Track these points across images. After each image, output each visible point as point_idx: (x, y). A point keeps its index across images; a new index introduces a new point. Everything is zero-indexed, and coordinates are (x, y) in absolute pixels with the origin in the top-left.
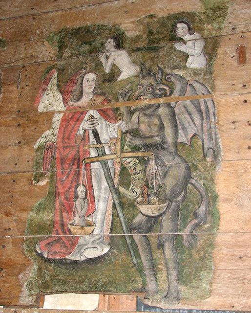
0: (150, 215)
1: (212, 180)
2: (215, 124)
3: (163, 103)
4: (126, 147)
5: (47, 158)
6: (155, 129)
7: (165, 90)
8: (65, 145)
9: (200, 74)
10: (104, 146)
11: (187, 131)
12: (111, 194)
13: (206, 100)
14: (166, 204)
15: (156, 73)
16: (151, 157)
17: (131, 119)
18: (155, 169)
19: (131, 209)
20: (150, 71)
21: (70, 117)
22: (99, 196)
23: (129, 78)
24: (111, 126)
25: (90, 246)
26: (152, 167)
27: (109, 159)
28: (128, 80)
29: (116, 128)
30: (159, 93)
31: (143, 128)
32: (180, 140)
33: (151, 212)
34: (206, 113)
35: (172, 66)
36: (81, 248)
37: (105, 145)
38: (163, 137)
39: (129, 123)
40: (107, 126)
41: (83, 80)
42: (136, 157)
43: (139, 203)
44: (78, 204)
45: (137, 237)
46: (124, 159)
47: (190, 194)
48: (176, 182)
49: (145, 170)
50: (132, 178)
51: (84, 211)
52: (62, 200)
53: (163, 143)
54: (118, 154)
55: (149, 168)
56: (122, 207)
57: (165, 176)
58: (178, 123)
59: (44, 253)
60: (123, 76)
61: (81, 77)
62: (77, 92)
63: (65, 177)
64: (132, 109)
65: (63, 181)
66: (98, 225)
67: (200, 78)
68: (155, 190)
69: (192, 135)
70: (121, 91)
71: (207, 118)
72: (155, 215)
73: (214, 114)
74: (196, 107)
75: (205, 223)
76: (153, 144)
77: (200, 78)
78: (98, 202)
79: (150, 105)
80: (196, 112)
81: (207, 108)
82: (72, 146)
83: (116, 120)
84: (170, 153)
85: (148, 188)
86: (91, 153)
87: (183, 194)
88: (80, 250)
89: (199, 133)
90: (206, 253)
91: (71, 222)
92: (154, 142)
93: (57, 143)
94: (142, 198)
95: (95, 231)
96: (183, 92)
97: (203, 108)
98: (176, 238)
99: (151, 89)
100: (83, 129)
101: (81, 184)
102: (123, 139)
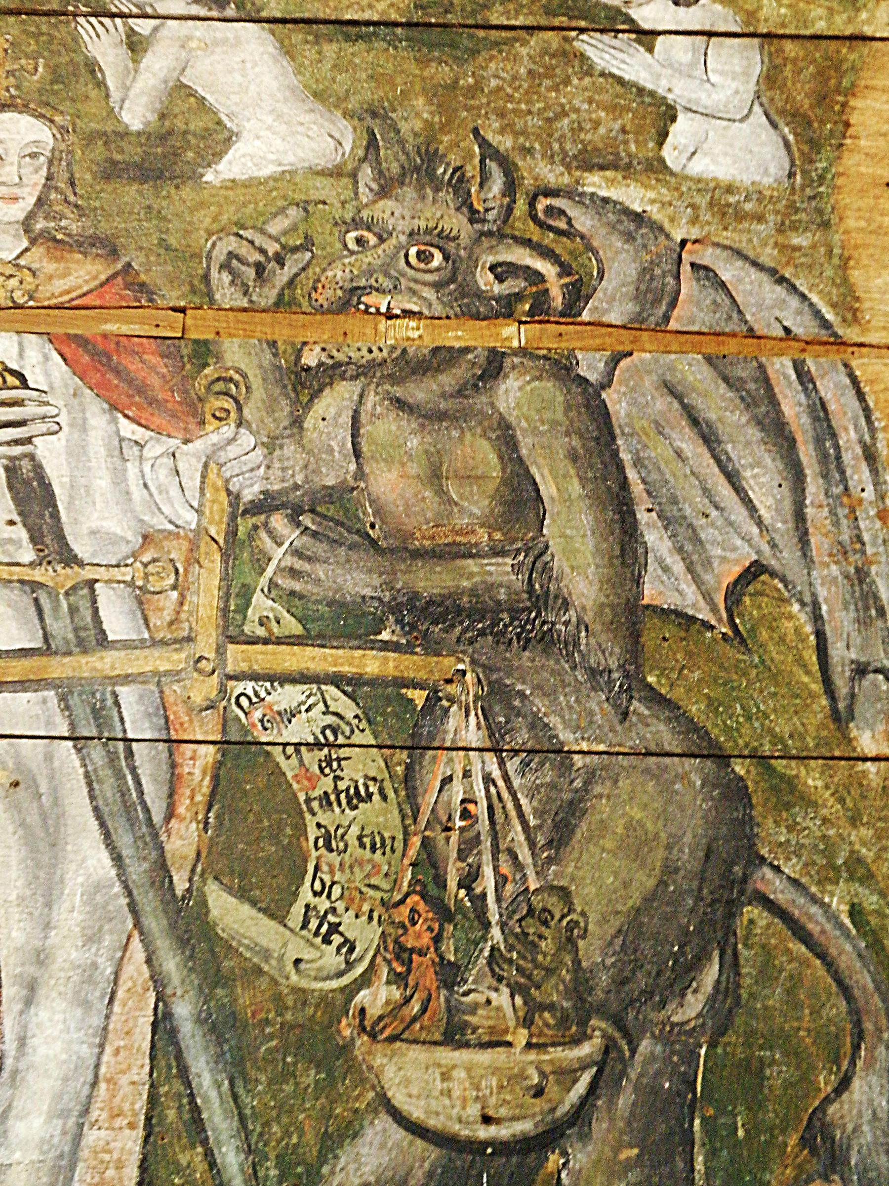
0: (465, 1133)
3: (522, 351)
4: (262, 604)
6: (474, 506)
7: (537, 277)
9: (760, 218)
10: (91, 584)
11: (696, 540)
12: (136, 944)
13: (811, 364)
14: (585, 1050)
15: (472, 170)
17: (297, 423)
18: (488, 780)
19: (310, 1077)
20: (431, 157)
23: (286, 177)
24: (153, 450)
26: (465, 770)
27: (127, 679)
28: (281, 189)
30: (497, 289)
32: (652, 592)
33: (474, 1111)
34: (819, 442)
35: (572, 149)
38: (537, 559)
39: (290, 448)
40: (120, 447)
42: (336, 680)
46: (249, 687)
48: (651, 883)
50: (312, 833)
54: (206, 645)
55: (442, 771)
56: (237, 1068)
57: (561, 828)
60: (232, 166)
64: (310, 359)
67: (759, 238)
68: (496, 933)
69: (737, 570)
70: (231, 244)
72: (503, 1132)
73: (870, 456)
74: (749, 402)
77: (759, 238)
78: (28, 1002)
79: (436, 350)
80: (754, 433)
81: (820, 412)
83: (192, 415)
84: (593, 673)
85: (445, 914)
87: (711, 973)
89: (787, 558)
94: (396, 994)
96: (655, 299)
97: (792, 406)
99: (438, 259)
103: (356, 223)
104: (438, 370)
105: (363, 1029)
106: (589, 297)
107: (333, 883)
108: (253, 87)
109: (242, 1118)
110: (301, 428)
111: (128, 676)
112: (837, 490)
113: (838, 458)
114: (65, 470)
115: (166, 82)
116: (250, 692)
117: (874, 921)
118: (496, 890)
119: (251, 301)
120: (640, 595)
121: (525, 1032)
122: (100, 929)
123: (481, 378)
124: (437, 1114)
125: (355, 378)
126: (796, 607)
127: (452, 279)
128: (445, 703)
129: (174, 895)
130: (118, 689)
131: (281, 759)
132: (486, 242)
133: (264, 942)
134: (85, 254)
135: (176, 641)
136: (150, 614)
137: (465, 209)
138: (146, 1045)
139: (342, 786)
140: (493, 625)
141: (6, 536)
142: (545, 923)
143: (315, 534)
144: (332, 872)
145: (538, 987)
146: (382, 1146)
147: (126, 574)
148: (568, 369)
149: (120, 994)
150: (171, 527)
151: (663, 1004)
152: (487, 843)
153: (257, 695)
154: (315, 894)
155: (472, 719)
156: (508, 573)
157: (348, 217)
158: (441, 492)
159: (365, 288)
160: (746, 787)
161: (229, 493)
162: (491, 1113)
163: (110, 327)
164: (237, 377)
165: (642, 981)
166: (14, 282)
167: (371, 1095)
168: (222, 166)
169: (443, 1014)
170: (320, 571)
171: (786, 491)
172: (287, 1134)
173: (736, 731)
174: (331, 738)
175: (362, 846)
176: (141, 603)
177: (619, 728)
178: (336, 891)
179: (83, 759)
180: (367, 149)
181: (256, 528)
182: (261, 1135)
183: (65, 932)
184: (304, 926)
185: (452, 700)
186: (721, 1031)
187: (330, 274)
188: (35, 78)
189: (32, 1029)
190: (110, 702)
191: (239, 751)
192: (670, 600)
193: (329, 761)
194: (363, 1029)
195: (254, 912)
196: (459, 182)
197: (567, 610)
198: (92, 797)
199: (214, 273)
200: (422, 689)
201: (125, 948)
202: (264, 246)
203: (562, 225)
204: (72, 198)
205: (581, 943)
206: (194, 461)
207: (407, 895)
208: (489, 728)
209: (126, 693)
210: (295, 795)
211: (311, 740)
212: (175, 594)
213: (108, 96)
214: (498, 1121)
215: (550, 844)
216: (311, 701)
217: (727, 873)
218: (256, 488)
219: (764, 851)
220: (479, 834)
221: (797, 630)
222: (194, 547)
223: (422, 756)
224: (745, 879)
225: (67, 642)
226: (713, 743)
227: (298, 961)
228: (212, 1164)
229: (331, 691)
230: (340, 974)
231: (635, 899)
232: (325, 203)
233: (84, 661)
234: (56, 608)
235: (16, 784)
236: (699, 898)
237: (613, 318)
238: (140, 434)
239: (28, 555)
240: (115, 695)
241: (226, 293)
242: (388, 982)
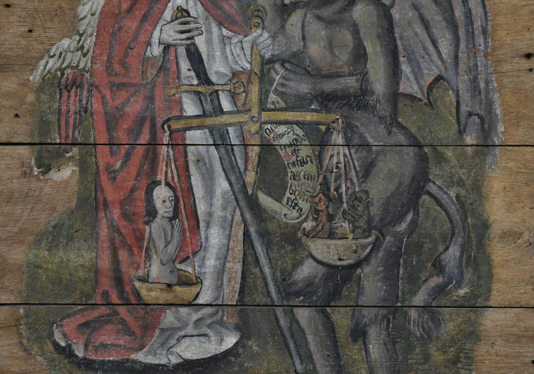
0: (334, 263)
1: (477, 188)
2: (486, 56)
4: (272, 97)
5: (69, 112)
6: (344, 57)
8: (117, 80)
10: (217, 91)
12: (238, 210)
14: (370, 239)
16: (335, 125)
17: (283, 27)
18: (345, 156)
19: (289, 248)
22: (210, 214)
24: (234, 40)
25: (190, 330)
26: (338, 153)
27: (230, 125)
29: (247, 46)
31: (315, 50)
32: (403, 88)
33: (336, 257)
36: (170, 336)
37: (219, 88)
38: (364, 77)
39: (281, 38)
40: (224, 40)
42: (297, 123)
43: (307, 234)
44: (156, 229)
45: (303, 315)
46: (269, 126)
47: (427, 217)
48: (394, 188)
49: (320, 158)
50: (290, 174)
51: (171, 248)
52: (116, 217)
53: (365, 91)
54: (255, 112)
55: (330, 153)
57: (367, 171)
59: (74, 347)
63: (119, 164)
65: (114, 172)
66: (208, 282)
68: (345, 205)
69: (431, 79)
71: (467, 41)
72: (344, 263)
73: (484, 32)
75: (459, 285)
76: (339, 93)
80: (444, 24)
81: (468, 14)
82: (135, 85)
84: (381, 118)
86: (185, 106)
87: (410, 217)
88: (167, 340)
89: (450, 74)
90: (460, 350)
91: (141, 273)
92: (342, 90)
93: (92, 72)
94: (314, 224)
95: (200, 296)
97: (459, 13)
98: (394, 318)
100: (160, 43)
101: (163, 182)
102: (264, 78)
105: (304, 234)
107: (296, 190)
109: (270, 259)
111: (230, 123)
112: (471, 46)
113: (473, 33)
114: (205, 49)
116: (269, 128)
117: (463, 199)
118: (346, 192)
120: (398, 89)
121: (352, 235)
122: (227, 206)
123: (347, 5)
124: (326, 258)
125: (303, 8)
126: (451, 92)
128: (332, 130)
129: (248, 195)
130: (228, 128)
131: (280, 150)
133: (275, 209)
135: (246, 111)
136: (237, 102)
138: (242, 240)
139: (299, 159)
140: (348, 102)
141: (188, 75)
142: (360, 202)
143: (290, 70)
144: (296, 187)
145: (357, 221)
146: (310, 267)
147: (228, 87)
149: (234, 225)
150: (241, 70)
151: (394, 226)
152: (343, 177)
153: (272, 129)
154: (291, 194)
155: (340, 136)
156: (353, 83)
158: (332, 53)
160: (427, 156)
161: (261, 56)
162: (341, 258)
164: (262, 9)
165: (389, 219)
167: (307, 253)
169: (328, 230)
170: (291, 84)
171: (452, 48)
172: (283, 264)
173: (425, 138)
174: (295, 143)
175: (305, 178)
176: (233, 97)
177: (388, 137)
178: (297, 193)
179: (218, 152)
181: (270, 69)
182: (275, 264)
183: (216, 207)
184: (287, 204)
185: (334, 129)
186: (411, 233)
189: (209, 235)
190: (225, 132)
191: (267, 147)
192: (409, 91)
193: (295, 150)
194: (304, 234)
195: (272, 200)
197: (373, 96)
198: (222, 164)
200: (325, 125)
201: (235, 211)
205: (371, 208)
206: (248, 43)
207: (318, 194)
208: (346, 138)
209: (231, 130)
210: (284, 162)
211: (289, 143)
212: (244, 94)
214: (343, 260)
215: (363, 176)
216: (289, 131)
217: (419, 185)
218: (269, 54)
219: (431, 177)
220: (341, 174)
221: (450, 100)
222: (249, 78)
223: (324, 148)
224: (424, 187)
225: (211, 112)
226: (418, 142)
227: (285, 215)
228: (262, 272)
229: (295, 127)
230: (298, 218)
231: (389, 194)
233: (216, 119)
234: (206, 100)
235: (198, 161)
236: (409, 193)
238: (230, 34)
239: (195, 82)
240: (227, 130)
242: (312, 221)
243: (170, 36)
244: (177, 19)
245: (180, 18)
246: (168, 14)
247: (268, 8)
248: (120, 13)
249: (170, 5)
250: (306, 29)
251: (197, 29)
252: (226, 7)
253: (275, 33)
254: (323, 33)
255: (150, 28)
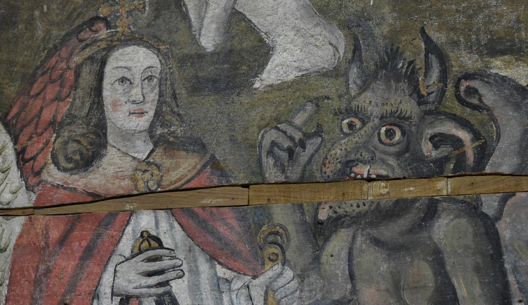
3: (450, 199)
7: (457, 143)
15: (420, 63)
17: (317, 259)
20: (394, 54)
21: (55, 234)
23: (303, 80)
24: (237, 285)
29: (257, 293)
30: (434, 154)
35: (484, 39)
39: (313, 278)
40: (219, 285)
41: (100, 77)
58: (514, 287)
60: (272, 74)
61: (91, 58)
62: (79, 130)
64: (323, 215)
70: (272, 135)
79: (397, 202)
99: (398, 136)
100: (113, 294)
103: (350, 112)
104: (398, 216)
106: (490, 155)
108: (280, 9)
110: (319, 263)
115: (225, 10)
119: (286, 177)
123: (423, 219)
125: (349, 226)
127: (407, 149)
132: (429, 119)
134: (187, 151)
137: (415, 95)
148: (476, 208)
157: (344, 107)
159: (353, 161)
163: (206, 201)
164: (281, 231)
166: (147, 175)
168: (264, 76)
180: (354, 52)
187: (333, 152)
188: (145, 15)
196: (411, 77)
199: (264, 159)
202: (293, 135)
203: (475, 101)
204: (176, 109)
213: (190, 26)
232: (328, 98)
237: (505, 169)
241: (272, 174)
243: (130, 282)
244: (141, 252)
245: (147, 250)
246: (126, 246)
247: (291, 228)
248: (47, 245)
249: (129, 229)
250: (354, 262)
251: (174, 267)
252: (222, 229)
253: (303, 271)
254: (384, 267)
255: (96, 269)
